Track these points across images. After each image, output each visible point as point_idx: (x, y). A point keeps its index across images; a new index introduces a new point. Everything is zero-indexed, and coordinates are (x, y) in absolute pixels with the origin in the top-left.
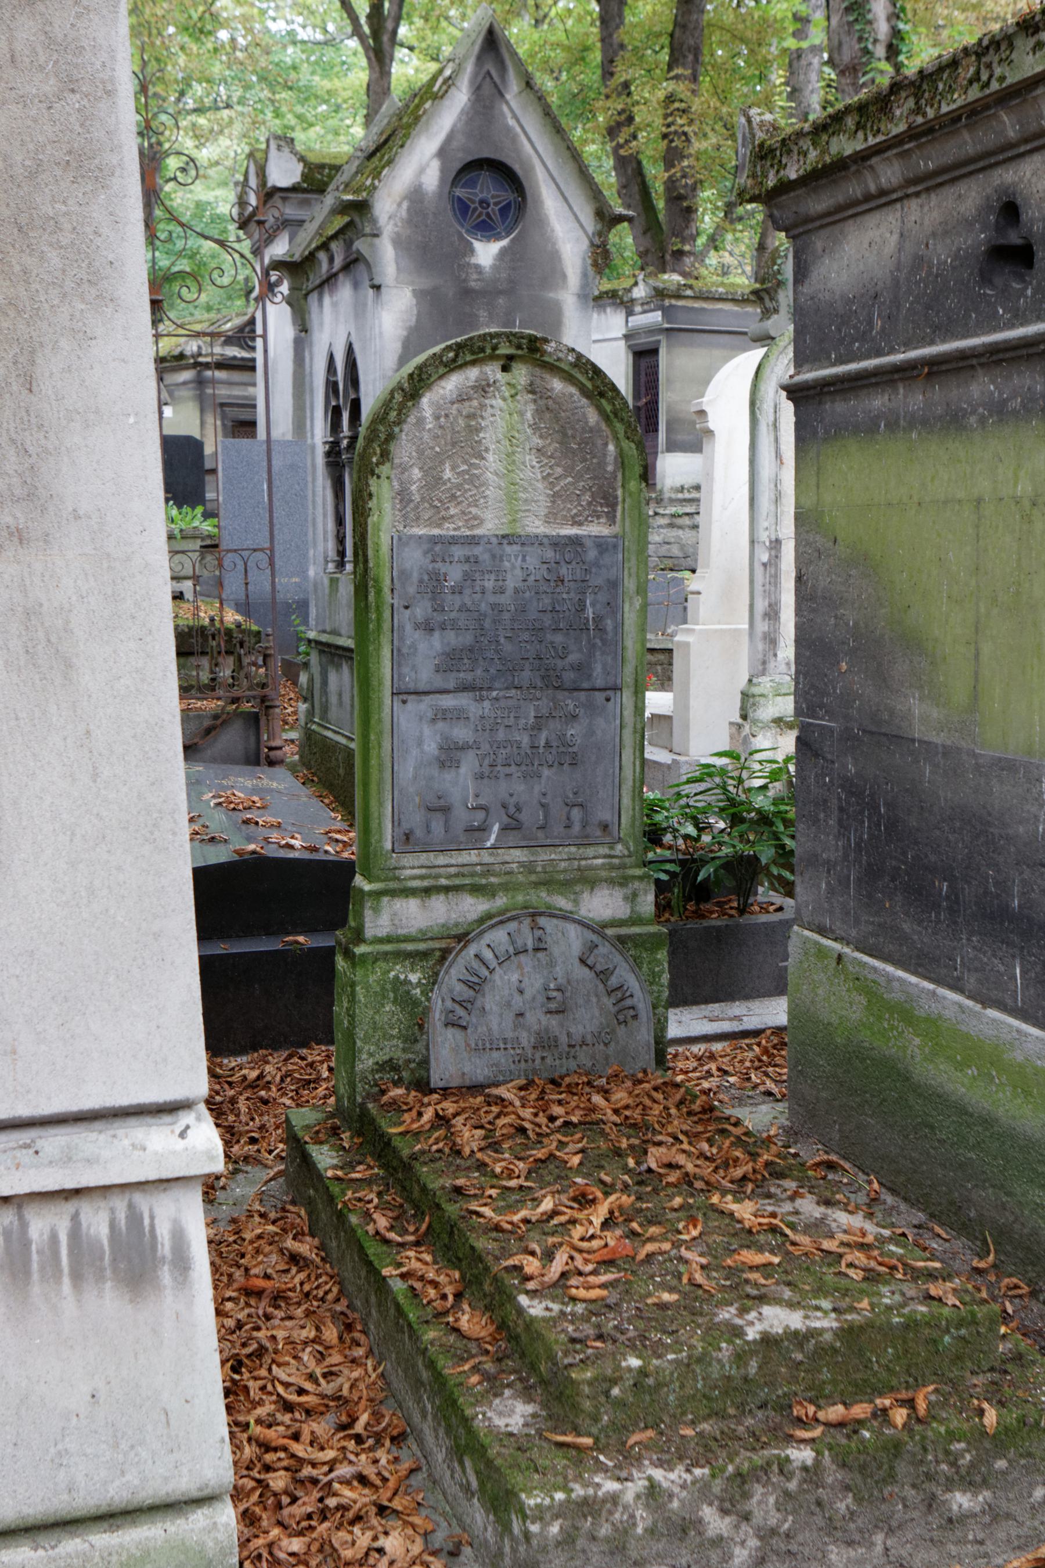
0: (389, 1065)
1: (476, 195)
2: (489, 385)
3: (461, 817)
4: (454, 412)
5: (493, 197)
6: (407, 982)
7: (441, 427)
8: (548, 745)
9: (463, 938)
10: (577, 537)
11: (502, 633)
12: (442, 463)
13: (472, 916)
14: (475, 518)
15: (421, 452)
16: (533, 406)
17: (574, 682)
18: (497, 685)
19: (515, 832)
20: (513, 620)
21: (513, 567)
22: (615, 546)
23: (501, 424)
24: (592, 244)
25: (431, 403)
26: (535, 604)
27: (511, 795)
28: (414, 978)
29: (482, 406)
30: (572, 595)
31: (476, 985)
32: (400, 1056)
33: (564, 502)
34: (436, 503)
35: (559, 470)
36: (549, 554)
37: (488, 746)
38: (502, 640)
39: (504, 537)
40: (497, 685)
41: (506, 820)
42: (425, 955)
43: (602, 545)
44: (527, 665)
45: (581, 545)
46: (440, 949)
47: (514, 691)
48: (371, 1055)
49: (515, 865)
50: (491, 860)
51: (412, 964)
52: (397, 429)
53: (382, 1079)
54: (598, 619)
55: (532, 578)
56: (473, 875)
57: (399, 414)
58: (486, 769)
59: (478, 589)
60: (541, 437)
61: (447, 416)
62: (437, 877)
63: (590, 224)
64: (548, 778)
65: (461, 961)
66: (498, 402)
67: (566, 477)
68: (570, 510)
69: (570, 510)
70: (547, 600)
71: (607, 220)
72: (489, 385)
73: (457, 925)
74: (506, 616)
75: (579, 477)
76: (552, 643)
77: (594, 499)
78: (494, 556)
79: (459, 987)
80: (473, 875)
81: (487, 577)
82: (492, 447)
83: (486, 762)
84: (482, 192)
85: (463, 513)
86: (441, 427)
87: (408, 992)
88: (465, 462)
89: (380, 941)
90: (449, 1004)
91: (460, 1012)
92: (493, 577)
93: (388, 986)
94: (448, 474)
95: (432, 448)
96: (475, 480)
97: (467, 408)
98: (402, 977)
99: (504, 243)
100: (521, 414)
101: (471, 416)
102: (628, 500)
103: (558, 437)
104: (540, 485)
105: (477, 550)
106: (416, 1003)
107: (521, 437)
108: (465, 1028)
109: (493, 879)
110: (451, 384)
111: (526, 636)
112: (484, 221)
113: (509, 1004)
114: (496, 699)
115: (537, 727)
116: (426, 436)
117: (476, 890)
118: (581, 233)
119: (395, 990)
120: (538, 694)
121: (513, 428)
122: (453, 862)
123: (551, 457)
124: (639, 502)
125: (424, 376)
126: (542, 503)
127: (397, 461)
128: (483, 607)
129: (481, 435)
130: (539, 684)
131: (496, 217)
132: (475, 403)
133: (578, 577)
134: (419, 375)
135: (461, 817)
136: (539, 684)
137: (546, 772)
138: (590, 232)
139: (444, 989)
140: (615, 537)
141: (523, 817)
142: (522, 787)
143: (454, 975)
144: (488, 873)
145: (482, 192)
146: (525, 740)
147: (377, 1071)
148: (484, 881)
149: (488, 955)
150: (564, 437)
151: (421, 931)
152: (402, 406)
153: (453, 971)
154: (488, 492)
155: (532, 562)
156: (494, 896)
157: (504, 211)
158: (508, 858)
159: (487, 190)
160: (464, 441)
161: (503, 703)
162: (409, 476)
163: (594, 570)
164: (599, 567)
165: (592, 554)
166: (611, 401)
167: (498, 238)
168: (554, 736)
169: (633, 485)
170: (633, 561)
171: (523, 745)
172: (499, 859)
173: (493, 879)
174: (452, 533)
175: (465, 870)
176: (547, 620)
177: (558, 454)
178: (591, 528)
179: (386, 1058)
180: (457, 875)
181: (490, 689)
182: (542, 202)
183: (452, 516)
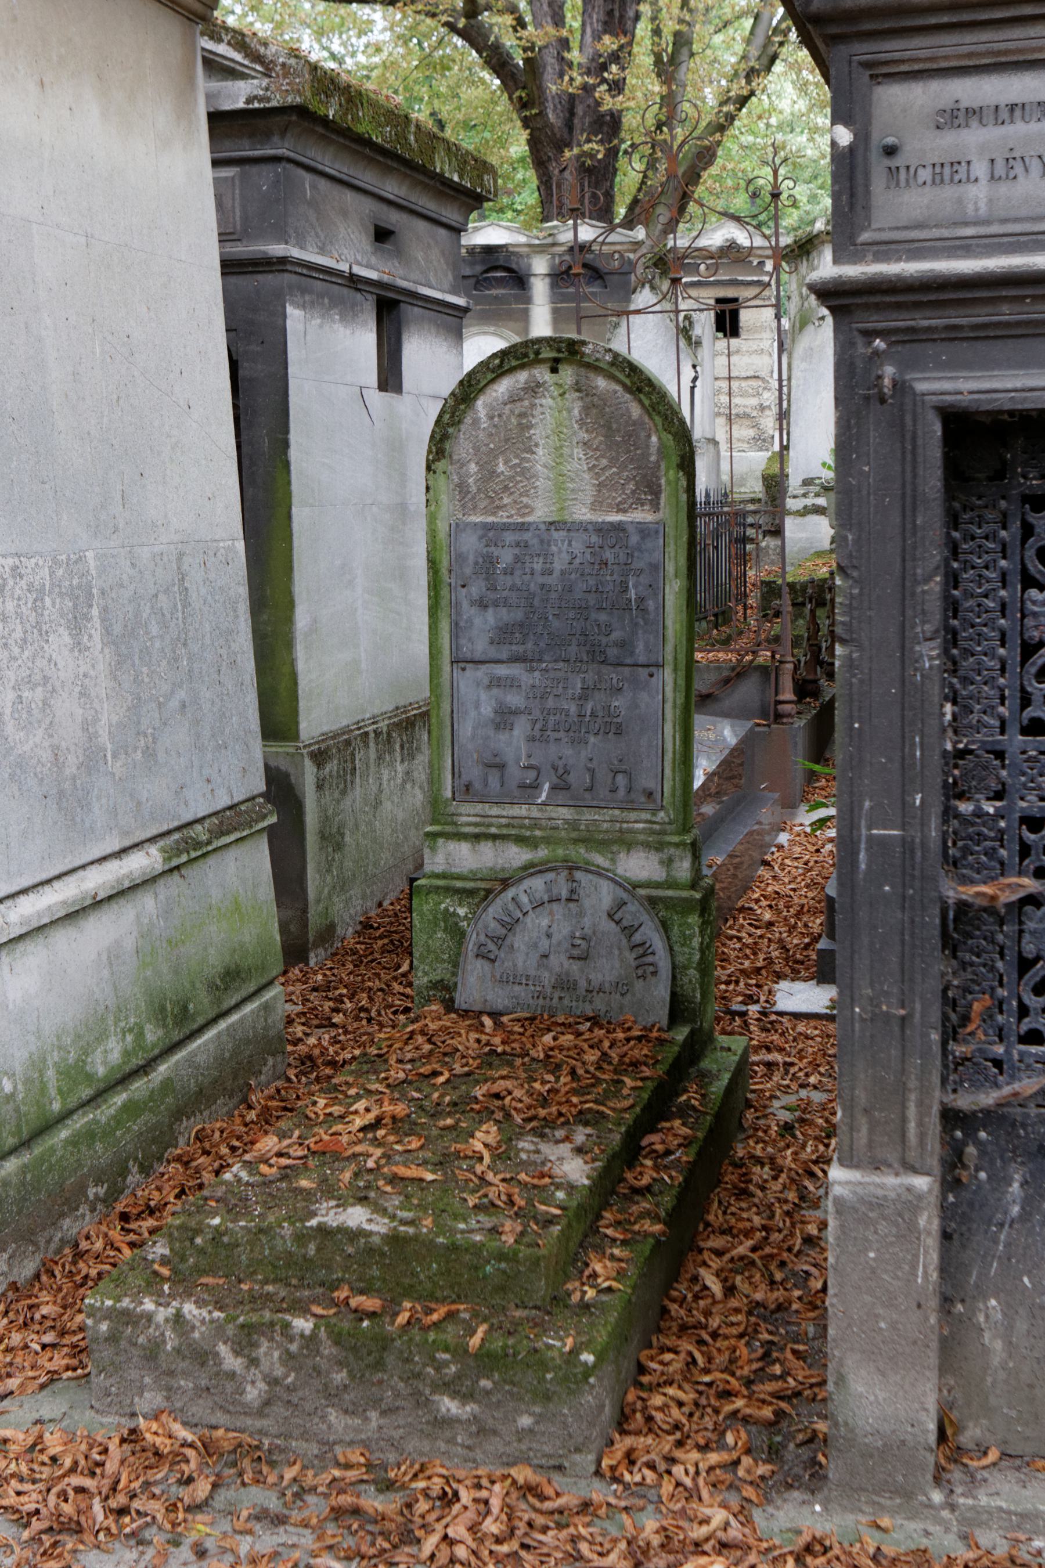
3: (515, 774)
8: (593, 714)
10: (620, 523)
12: (496, 457)
14: (526, 506)
15: (477, 449)
20: (560, 599)
21: (560, 551)
25: (485, 405)
29: (533, 406)
31: (510, 925)
36: (594, 539)
43: (644, 530)
45: (624, 530)
54: (641, 599)
55: (577, 561)
56: (521, 827)
58: (537, 733)
62: (490, 825)
66: (547, 401)
70: (592, 582)
73: (503, 870)
74: (553, 595)
75: (623, 467)
78: (542, 541)
79: (493, 924)
80: (521, 827)
82: (542, 442)
83: (538, 726)
88: (517, 456)
90: (482, 938)
91: (491, 946)
96: (524, 472)
97: (518, 408)
101: (522, 415)
104: (586, 476)
105: (527, 536)
108: (493, 961)
110: (503, 387)
113: (535, 945)
114: (546, 670)
115: (584, 697)
117: (520, 840)
120: (584, 667)
126: (588, 493)
132: (526, 403)
135: (515, 774)
149: (524, 899)
150: (608, 430)
155: (578, 547)
160: (516, 437)
161: (552, 674)
164: (640, 551)
165: (634, 539)
166: (648, 395)
175: (515, 822)
180: (507, 826)
181: (540, 661)
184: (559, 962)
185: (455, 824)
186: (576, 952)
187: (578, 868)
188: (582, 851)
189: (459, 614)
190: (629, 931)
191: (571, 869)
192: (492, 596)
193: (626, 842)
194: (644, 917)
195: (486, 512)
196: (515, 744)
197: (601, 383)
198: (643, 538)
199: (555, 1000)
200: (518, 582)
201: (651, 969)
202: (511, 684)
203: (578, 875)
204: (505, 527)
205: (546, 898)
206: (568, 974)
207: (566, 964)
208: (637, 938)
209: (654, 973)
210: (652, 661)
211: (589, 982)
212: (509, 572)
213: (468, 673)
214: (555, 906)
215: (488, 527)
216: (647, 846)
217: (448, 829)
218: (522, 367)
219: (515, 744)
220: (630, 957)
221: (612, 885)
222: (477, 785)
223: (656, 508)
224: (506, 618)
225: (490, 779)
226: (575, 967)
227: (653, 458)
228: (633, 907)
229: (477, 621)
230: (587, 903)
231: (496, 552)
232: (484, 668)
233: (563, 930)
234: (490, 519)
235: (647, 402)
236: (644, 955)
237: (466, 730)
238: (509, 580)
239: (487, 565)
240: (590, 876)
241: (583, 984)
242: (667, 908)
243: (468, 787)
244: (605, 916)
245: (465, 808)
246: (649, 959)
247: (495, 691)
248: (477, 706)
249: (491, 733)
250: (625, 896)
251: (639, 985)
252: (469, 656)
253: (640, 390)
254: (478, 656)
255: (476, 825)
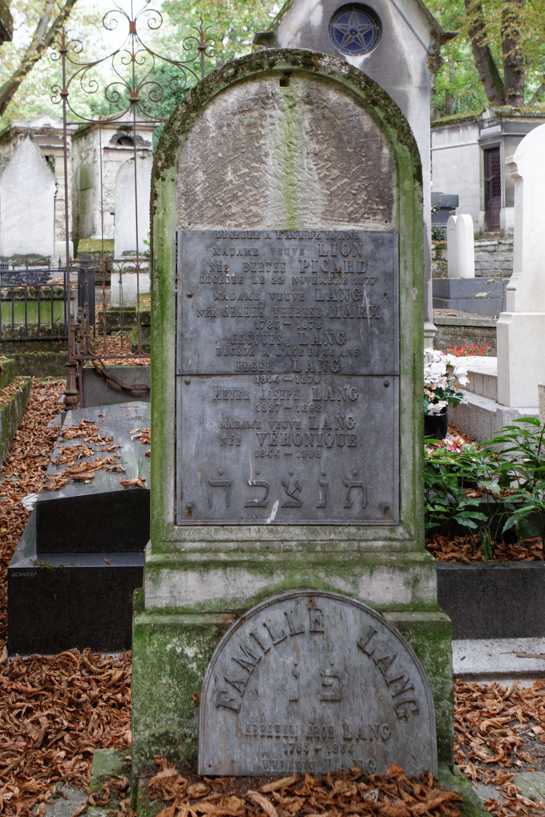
0: (164, 739)
1: (348, 27)
2: (268, 98)
3: (242, 494)
4: (236, 122)
5: (359, 27)
6: (183, 655)
7: (223, 135)
8: (327, 428)
9: (240, 614)
10: (353, 232)
11: (281, 321)
12: (224, 166)
13: (250, 592)
14: (256, 215)
15: (204, 158)
16: (310, 116)
17: (352, 368)
18: (276, 369)
19: (295, 510)
20: (292, 308)
21: (292, 260)
22: (391, 241)
23: (280, 131)
24: (429, 54)
25: (214, 114)
26: (313, 294)
27: (291, 474)
28: (190, 652)
29: (262, 117)
30: (349, 286)
32: (176, 730)
33: (340, 200)
34: (219, 202)
35: (336, 172)
36: (327, 248)
37: (268, 427)
38: (281, 327)
39: (282, 232)
40: (276, 369)
41: (286, 498)
42: (201, 629)
43: (378, 240)
44: (306, 352)
45: (357, 239)
46: (217, 625)
47: (293, 375)
48: (148, 726)
49: (294, 544)
50: (270, 537)
51: (189, 638)
52: (181, 138)
53: (157, 752)
54: (375, 309)
55: (310, 270)
56: (252, 551)
57: (183, 124)
58: (266, 449)
59: (257, 280)
60: (318, 142)
61: (229, 125)
62: (217, 551)
63: (427, 41)
64: (328, 459)
65: (235, 639)
66: (277, 113)
67: (342, 178)
68: (346, 208)
69: (346, 208)
70: (325, 291)
71: (441, 37)
72: (268, 98)
73: (234, 600)
74: (285, 305)
75: (355, 178)
76: (329, 330)
77: (369, 198)
78: (273, 250)
80: (252, 551)
81: (266, 268)
82: (271, 152)
83: (267, 442)
84: (351, 24)
85: (244, 211)
86: (223, 135)
87: (184, 666)
88: (246, 166)
89: (167, 611)
92: (272, 269)
93: (165, 659)
94: (230, 176)
95: (216, 154)
96: (255, 182)
97: (247, 119)
98: (179, 650)
99: (367, 56)
100: (299, 122)
101: (250, 126)
102: (403, 198)
103: (334, 142)
104: (317, 186)
105: (257, 245)
106: (192, 678)
107: (299, 143)
109: (271, 557)
110: (233, 98)
111: (304, 324)
112: (353, 43)
114: (276, 382)
115: (316, 410)
116: (209, 143)
117: (254, 566)
118: (421, 47)
119: (172, 663)
120: (317, 378)
121: (291, 135)
122: (233, 537)
123: (327, 160)
124: (414, 200)
125: (206, 91)
126: (320, 203)
127: (182, 165)
128: (263, 296)
129: (261, 142)
130: (318, 369)
131: (362, 40)
132: (256, 114)
133: (355, 270)
134: (202, 89)
135: (242, 494)
136: (318, 369)
137: (325, 453)
138: (427, 46)
139: (218, 669)
140: (392, 232)
141: (303, 496)
142: (302, 467)
143: (230, 651)
144: (267, 550)
145: (351, 24)
146: (305, 422)
147: (154, 744)
148: (262, 558)
150: (339, 141)
151: (199, 604)
152: (185, 119)
153: (227, 649)
154: (268, 193)
155: (310, 255)
156: (271, 573)
157: (367, 36)
158: (287, 536)
159: (355, 23)
160: (246, 147)
161: (282, 386)
162: (194, 179)
163: (370, 263)
164: (375, 260)
165: (368, 248)
167: (363, 53)
168: (332, 419)
169: (407, 184)
170: (409, 255)
171: (302, 426)
172: (279, 537)
173: (271, 557)
174: (234, 229)
175: (245, 546)
176: (325, 309)
177: (334, 158)
178: (367, 225)
179: (162, 731)
180: (236, 550)
181: (270, 372)
182: (393, 29)
183: (234, 214)
184: (310, 706)
185: (178, 551)
186: (329, 694)
187: (319, 595)
188: (322, 575)
189: (185, 325)
190: (383, 664)
191: (311, 596)
192: (220, 306)
193: (368, 563)
194: (398, 647)
195: (213, 220)
196: (242, 462)
197: (333, 96)
198: (377, 247)
199: (311, 753)
200: (248, 292)
201: (412, 707)
202: (240, 397)
203: (320, 602)
204: (234, 236)
205: (287, 631)
206: (322, 720)
207: (319, 707)
208: (393, 671)
209: (416, 712)
210: (388, 371)
211: (345, 727)
212: (238, 281)
213: (192, 387)
214: (298, 639)
215: (217, 236)
216: (391, 566)
217: (173, 557)
218: (253, 78)
219: (242, 462)
220: (387, 694)
221: (358, 612)
222: (201, 507)
223: (388, 217)
224: (234, 329)
225: (215, 500)
226: (329, 711)
227: (385, 170)
228: (383, 636)
229: (204, 332)
230: (333, 634)
231: (224, 260)
232: (210, 381)
233: (310, 668)
234: (218, 228)
235: (382, 115)
236: (402, 692)
237: (189, 447)
238: (238, 290)
239: (216, 275)
240: (333, 603)
241: (339, 731)
242: (417, 634)
243: (190, 510)
244: (355, 648)
245: (189, 533)
246: (409, 696)
247: (222, 405)
248: (202, 421)
249: (217, 450)
250: (373, 623)
251: (401, 726)
252: (194, 369)
253: (375, 103)
254: (204, 369)
255: (202, 551)
